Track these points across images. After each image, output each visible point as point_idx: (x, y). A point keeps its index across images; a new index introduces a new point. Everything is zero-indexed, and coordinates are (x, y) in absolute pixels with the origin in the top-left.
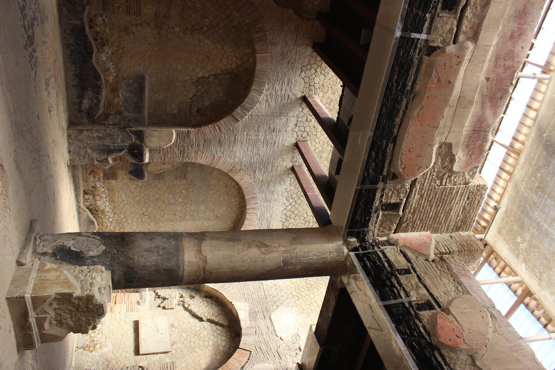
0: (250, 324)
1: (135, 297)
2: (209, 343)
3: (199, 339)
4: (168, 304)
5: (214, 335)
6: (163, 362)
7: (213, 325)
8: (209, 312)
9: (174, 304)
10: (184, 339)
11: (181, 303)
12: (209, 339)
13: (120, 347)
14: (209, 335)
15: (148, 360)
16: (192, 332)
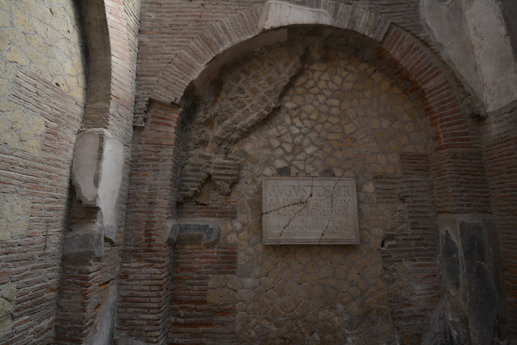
0: (325, 8)
2: (335, 106)
3: (323, 124)
4: (226, 175)
5: (316, 94)
7: (291, 92)
9: (227, 161)
11: (224, 146)
13: (332, 288)
15: (368, 228)
16: (305, 135)
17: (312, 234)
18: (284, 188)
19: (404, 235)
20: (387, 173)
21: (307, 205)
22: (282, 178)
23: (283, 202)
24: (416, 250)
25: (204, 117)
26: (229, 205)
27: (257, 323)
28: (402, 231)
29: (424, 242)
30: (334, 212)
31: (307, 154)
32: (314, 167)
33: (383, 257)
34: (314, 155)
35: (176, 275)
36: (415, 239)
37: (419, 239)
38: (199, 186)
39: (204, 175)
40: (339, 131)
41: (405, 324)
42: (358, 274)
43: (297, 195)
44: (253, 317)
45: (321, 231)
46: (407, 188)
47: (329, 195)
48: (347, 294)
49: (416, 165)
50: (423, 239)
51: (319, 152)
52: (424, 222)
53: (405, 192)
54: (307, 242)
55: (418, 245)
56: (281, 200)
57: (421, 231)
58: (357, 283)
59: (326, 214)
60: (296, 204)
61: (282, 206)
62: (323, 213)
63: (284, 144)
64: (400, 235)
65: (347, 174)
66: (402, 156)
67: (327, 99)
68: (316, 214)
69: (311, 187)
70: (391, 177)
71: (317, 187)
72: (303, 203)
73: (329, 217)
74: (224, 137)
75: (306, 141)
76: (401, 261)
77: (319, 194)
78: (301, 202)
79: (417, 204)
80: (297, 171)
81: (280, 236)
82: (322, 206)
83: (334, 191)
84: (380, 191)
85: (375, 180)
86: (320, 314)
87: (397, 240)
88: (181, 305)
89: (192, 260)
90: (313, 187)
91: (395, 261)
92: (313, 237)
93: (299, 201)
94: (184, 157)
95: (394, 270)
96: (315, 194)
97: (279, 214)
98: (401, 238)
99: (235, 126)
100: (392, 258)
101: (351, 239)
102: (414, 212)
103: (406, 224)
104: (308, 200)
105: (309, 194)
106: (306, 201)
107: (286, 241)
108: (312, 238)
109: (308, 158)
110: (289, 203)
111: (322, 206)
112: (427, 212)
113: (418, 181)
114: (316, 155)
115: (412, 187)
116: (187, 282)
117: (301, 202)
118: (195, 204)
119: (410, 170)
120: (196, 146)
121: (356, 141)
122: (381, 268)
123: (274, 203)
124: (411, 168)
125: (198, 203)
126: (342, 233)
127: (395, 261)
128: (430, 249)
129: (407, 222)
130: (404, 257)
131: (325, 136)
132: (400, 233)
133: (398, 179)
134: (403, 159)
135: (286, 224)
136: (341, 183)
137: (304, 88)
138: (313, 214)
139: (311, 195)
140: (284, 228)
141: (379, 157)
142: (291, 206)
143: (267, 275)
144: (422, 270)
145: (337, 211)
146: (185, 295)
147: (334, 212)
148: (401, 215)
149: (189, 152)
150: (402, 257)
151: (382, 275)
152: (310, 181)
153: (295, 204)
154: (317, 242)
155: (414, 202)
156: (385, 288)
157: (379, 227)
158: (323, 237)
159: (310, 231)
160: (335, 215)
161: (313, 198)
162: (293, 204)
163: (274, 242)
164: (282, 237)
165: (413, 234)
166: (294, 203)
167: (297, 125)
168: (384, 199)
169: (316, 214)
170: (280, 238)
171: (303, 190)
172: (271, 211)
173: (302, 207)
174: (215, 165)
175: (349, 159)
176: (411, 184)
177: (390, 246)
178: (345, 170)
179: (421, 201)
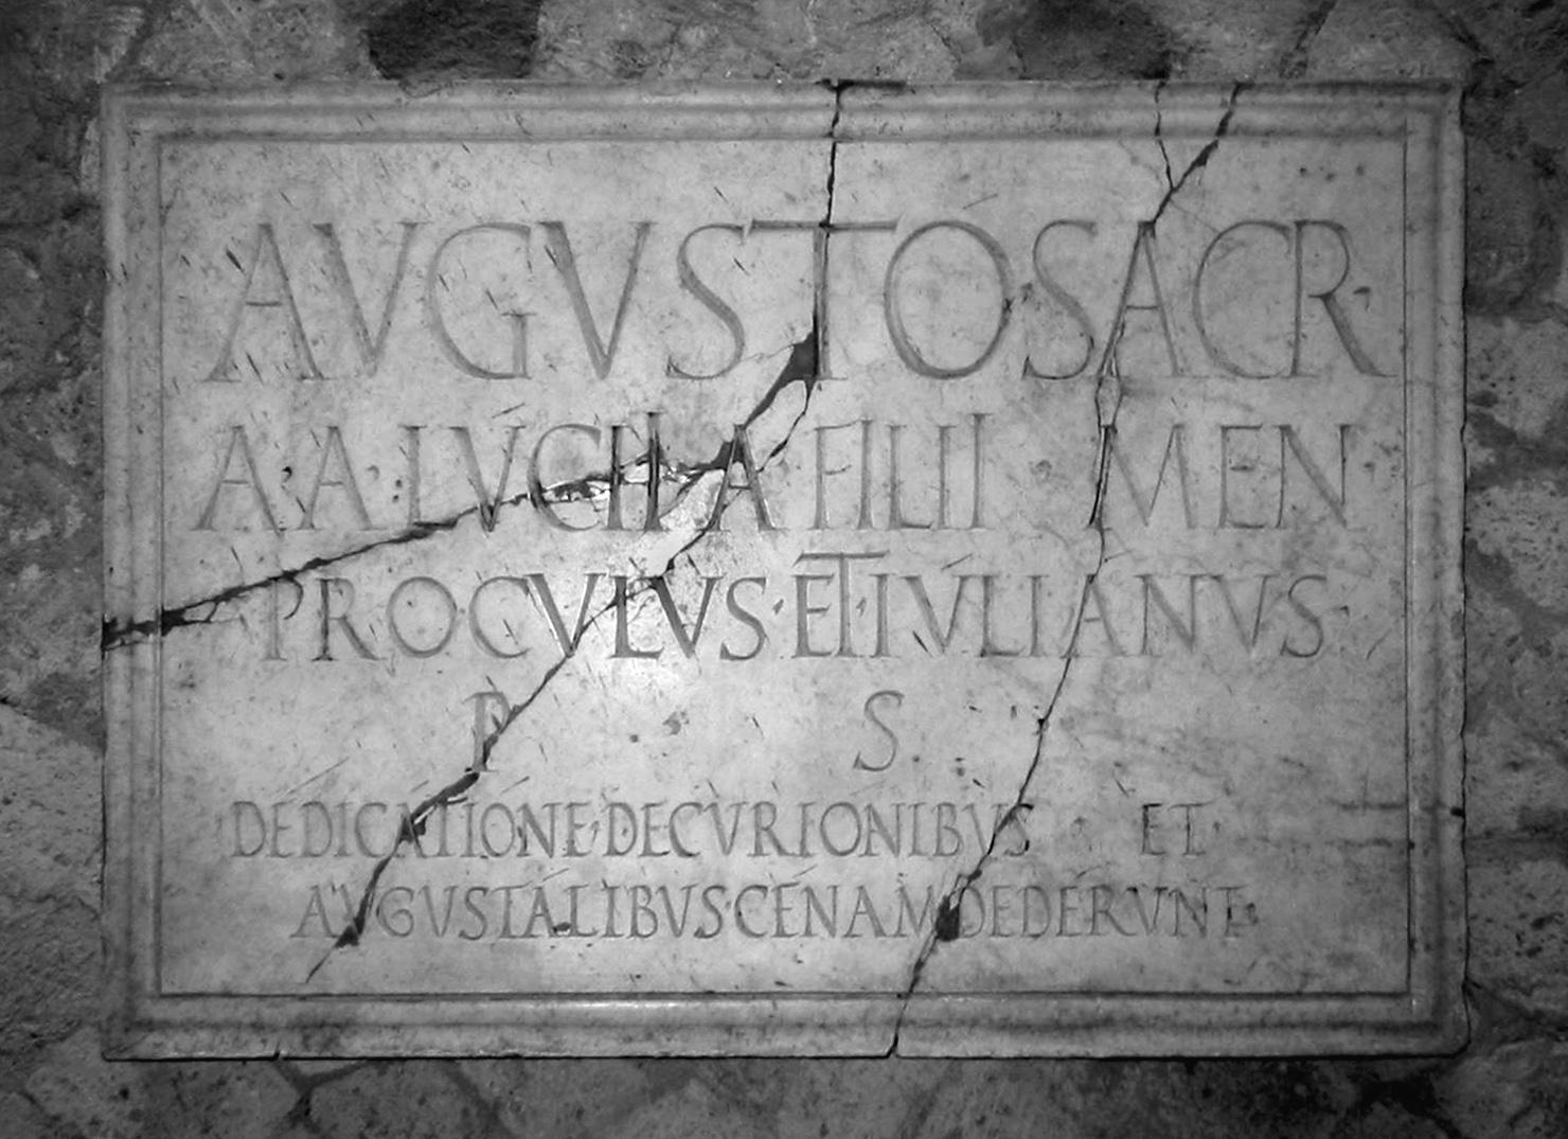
17: (794, 921)
21: (741, 509)
23: (395, 465)
30: (1122, 598)
43: (603, 359)
45: (928, 877)
47: (1064, 351)
54: (729, 1027)
59: (1011, 628)
62: (969, 621)
68: (863, 640)
69: (804, 242)
71: (889, 242)
73: (1047, 670)
77: (918, 336)
82: (959, 513)
83: (1143, 293)
90: (838, 243)
93: (632, 446)
97: (339, 641)
104: (760, 440)
105: (771, 344)
106: (735, 451)
108: (796, 978)
110: (491, 482)
111: (959, 513)
123: (272, 480)
135: (435, 789)
138: (824, 633)
139: (807, 363)
140: (411, 830)
142: (505, 512)
145: (1174, 592)
147: (1122, 598)
152: (794, 151)
154: (865, 1022)
158: (951, 960)
160: (1131, 640)
161: (835, 397)
162: (538, 496)
171: (689, 281)
172: (229, 595)
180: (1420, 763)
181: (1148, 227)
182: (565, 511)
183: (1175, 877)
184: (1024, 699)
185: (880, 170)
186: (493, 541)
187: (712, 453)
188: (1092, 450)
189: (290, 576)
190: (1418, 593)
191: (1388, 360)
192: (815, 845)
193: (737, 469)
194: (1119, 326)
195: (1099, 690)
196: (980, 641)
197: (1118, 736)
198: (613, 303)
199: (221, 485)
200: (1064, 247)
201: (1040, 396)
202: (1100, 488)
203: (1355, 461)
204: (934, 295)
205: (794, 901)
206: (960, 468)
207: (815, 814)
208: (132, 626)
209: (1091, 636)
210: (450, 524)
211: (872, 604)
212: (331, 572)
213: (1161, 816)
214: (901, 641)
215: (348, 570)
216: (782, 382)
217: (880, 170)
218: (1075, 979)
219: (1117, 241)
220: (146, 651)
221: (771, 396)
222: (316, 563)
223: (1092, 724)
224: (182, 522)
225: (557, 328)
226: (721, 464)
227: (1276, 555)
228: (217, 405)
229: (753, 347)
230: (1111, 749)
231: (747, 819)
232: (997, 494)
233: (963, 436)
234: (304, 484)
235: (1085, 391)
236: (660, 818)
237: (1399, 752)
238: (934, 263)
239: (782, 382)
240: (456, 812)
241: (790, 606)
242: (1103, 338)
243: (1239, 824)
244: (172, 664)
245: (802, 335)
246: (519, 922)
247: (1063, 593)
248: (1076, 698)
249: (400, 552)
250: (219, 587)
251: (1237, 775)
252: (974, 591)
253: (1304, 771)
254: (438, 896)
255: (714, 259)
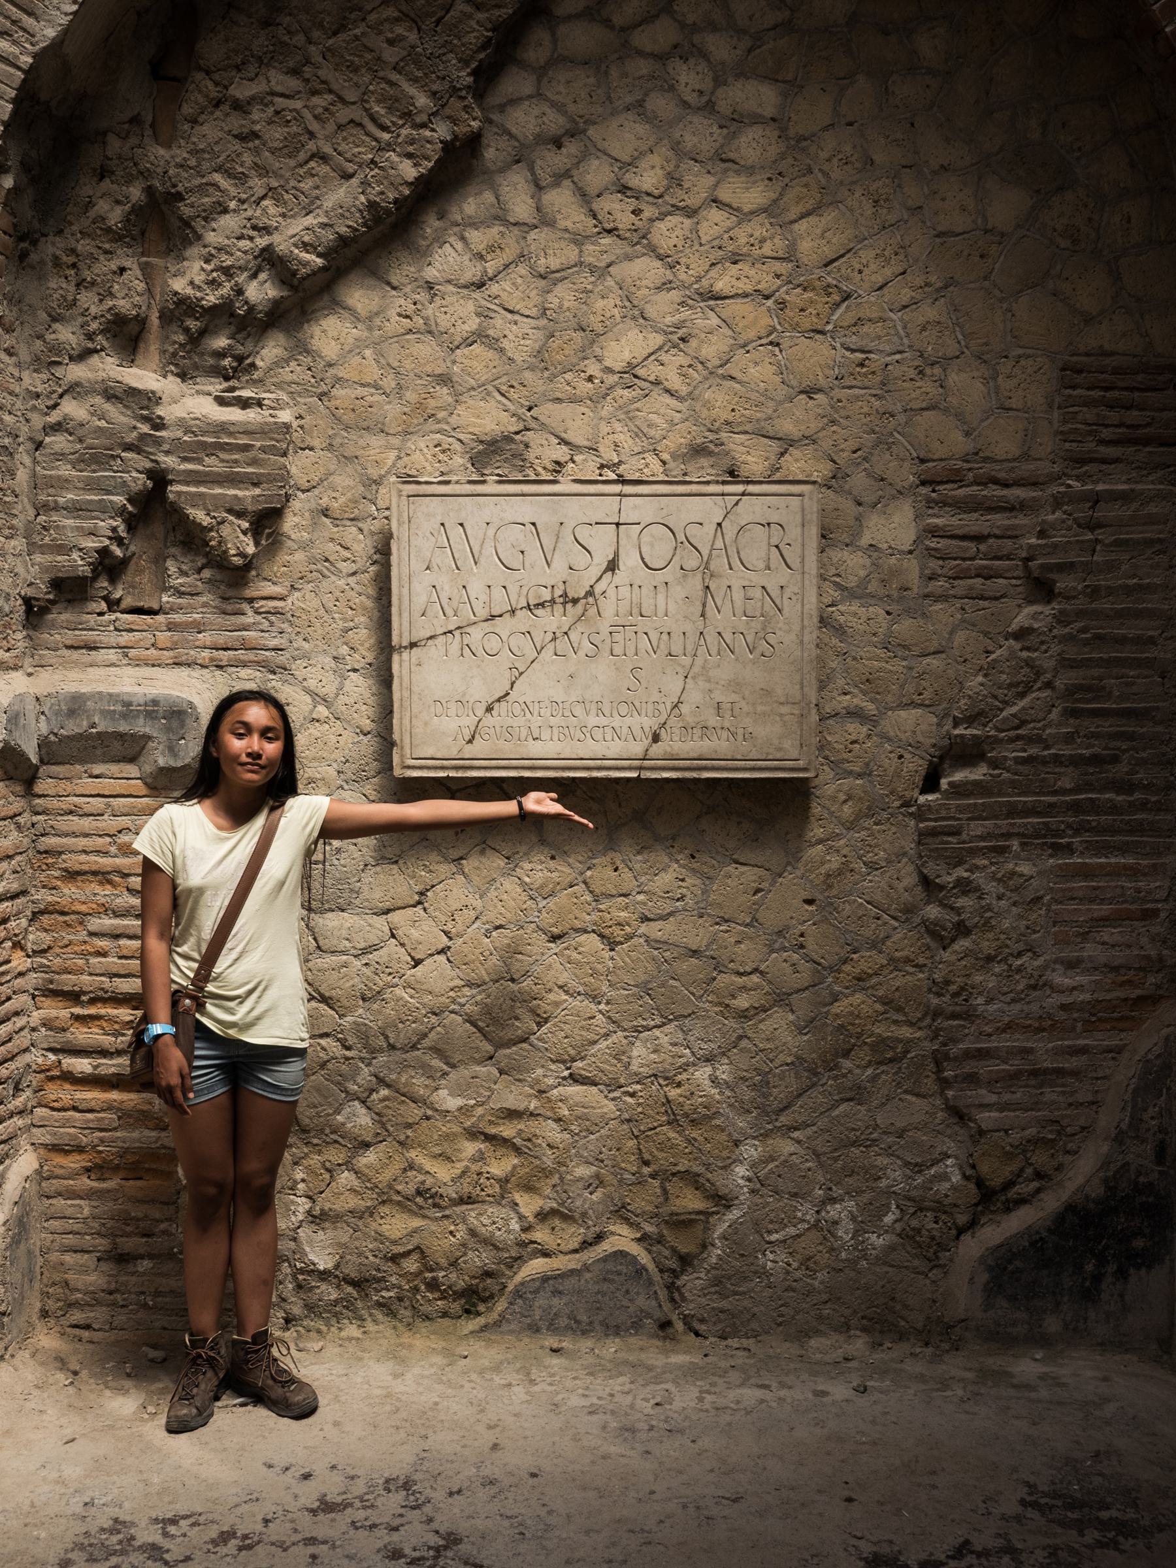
1: (98, 803)
3: (691, 213)
6: (912, 569)
7: (538, 46)
8: (391, 55)
9: (233, 414)
10: (675, 358)
12: (709, 108)
13: (695, 953)
14: (659, 103)
15: (870, 708)
17: (608, 737)
18: (491, 532)
19: (1030, 740)
20: (986, 459)
21: (592, 611)
22: (480, 488)
23: (484, 597)
24: (1076, 807)
25: (118, 202)
26: (250, 612)
27: (381, 1081)
28: (1023, 723)
29: (1121, 770)
30: (711, 638)
31: (609, 370)
32: (638, 434)
33: (923, 836)
34: (641, 372)
35: (50, 899)
36: (1075, 761)
37: (1095, 760)
38: (114, 529)
39: (135, 480)
40: (767, 249)
41: (993, 1098)
42: (809, 902)
44: (362, 1059)
45: (650, 723)
46: (1069, 529)
47: (693, 562)
48: (755, 978)
49: (1134, 416)
50: (1115, 760)
51: (664, 357)
52: (1127, 684)
53: (1055, 546)
55: (1088, 787)
56: (476, 588)
57: (1107, 726)
58: (802, 935)
59: (677, 648)
60: (541, 605)
61: (482, 613)
63: (498, 322)
64: (1012, 740)
65: (796, 464)
66: (1070, 373)
67: (719, 81)
68: (631, 651)
70: (1002, 475)
71: (638, 528)
72: (575, 601)
73: (686, 661)
74: (211, 298)
75: (607, 305)
76: (1002, 850)
78: (565, 595)
79: (1105, 605)
80: (562, 453)
81: (470, 742)
82: (661, 612)
84: (942, 544)
85: (924, 490)
86: (635, 1053)
87: (994, 764)
88: (78, 1010)
89: (108, 839)
91: (973, 852)
92: (614, 748)
93: (558, 592)
94: (38, 396)
95: (964, 887)
96: (629, 561)
98: (1012, 753)
99: (262, 242)
100: (964, 836)
101: (778, 756)
102: (1086, 643)
103: (1047, 693)
104: (598, 589)
105: (601, 560)
106: (590, 593)
107: (494, 763)
108: (609, 755)
109: (611, 388)
111: (661, 612)
112: (1152, 641)
113: (1124, 497)
114: (651, 371)
115: (1092, 526)
116: (95, 923)
117: (565, 595)
118: (103, 606)
119: (1102, 442)
120: (90, 345)
121: (852, 301)
122: (910, 878)
123: (445, 602)
124: (1106, 433)
125: (119, 601)
126: (740, 731)
127: (973, 852)
128: (1143, 806)
129: (1049, 685)
130: (1018, 834)
131: (699, 279)
132: (1012, 733)
133: (1034, 484)
134: (1074, 387)
135: (497, 696)
136: (753, 509)
137: (607, 23)
138: (618, 650)
139: (612, 566)
140: (489, 709)
141: (954, 378)
142: (518, 612)
143: (419, 903)
144: (1095, 888)
145: (728, 636)
146: (91, 974)
147: (711, 638)
148: (1025, 654)
149: (59, 372)
150: (1008, 836)
151: (909, 910)
153: (537, 605)
154: (630, 768)
155: (1094, 593)
156: (921, 961)
157: (922, 705)
158: (657, 750)
159: (602, 721)
160: (714, 651)
161: (621, 576)
162: (529, 607)
163: (443, 768)
164: (479, 748)
165: (1069, 739)
166: (532, 603)
167: (562, 224)
168: (956, 583)
169: (631, 651)
170: (470, 750)
172: (431, 638)
173: (566, 622)
174: (179, 434)
175: (809, 392)
176: (1092, 507)
177: (958, 790)
178: (787, 443)
179: (1128, 590)
180: (805, 689)
181: (719, 525)
182: (536, 612)
183: (726, 724)
184: (679, 669)
185: (635, 507)
186: (514, 621)
187: (582, 594)
188: (701, 593)
189: (450, 632)
190: (806, 639)
191: (795, 564)
192: (615, 714)
193: (591, 600)
194: (710, 555)
195: (703, 668)
196: (666, 652)
197: (709, 681)
198: (552, 547)
199: (430, 602)
200: (693, 531)
201: (685, 576)
202: (704, 605)
203: (786, 596)
204: (652, 545)
205: (609, 731)
206: (661, 598)
207: (615, 705)
208: (401, 647)
209: (702, 650)
210: (500, 616)
211: (634, 640)
212: (463, 630)
213: (723, 706)
214: (642, 652)
215: (468, 630)
216: (605, 572)
217: (635, 507)
218: (695, 755)
219: (710, 528)
220: (405, 655)
221: (601, 577)
222: (459, 628)
223: (701, 678)
224: (416, 614)
225: (535, 555)
226: (585, 597)
227: (759, 627)
228: (428, 578)
229: (596, 560)
230: (708, 686)
231: (594, 706)
232: (672, 607)
233: (661, 589)
234: (455, 603)
235: (699, 576)
236: (567, 705)
237: (798, 687)
238: (652, 536)
239: (605, 572)
240: (503, 704)
241: (608, 641)
242: (705, 559)
243: (746, 709)
244: (413, 660)
245: (611, 557)
246: (523, 737)
247: (692, 638)
248: (696, 669)
249: (486, 624)
250: (428, 635)
251: (747, 693)
252: (665, 637)
253: (767, 692)
254: (498, 729)
255: (583, 534)
